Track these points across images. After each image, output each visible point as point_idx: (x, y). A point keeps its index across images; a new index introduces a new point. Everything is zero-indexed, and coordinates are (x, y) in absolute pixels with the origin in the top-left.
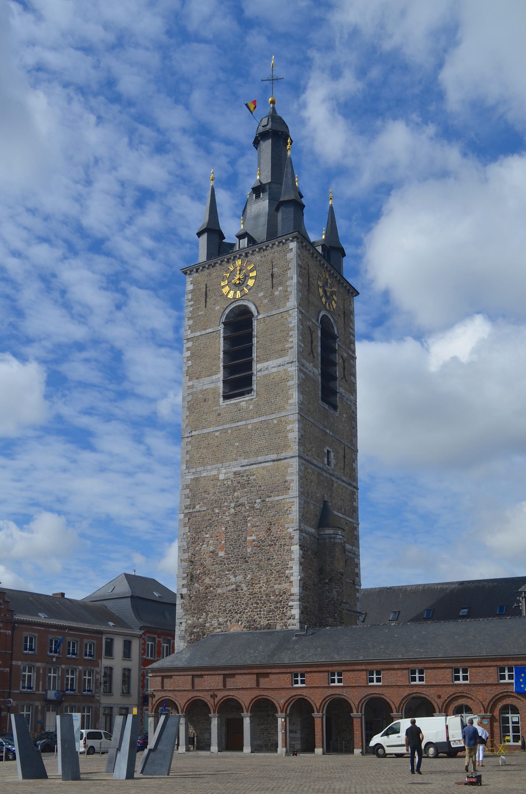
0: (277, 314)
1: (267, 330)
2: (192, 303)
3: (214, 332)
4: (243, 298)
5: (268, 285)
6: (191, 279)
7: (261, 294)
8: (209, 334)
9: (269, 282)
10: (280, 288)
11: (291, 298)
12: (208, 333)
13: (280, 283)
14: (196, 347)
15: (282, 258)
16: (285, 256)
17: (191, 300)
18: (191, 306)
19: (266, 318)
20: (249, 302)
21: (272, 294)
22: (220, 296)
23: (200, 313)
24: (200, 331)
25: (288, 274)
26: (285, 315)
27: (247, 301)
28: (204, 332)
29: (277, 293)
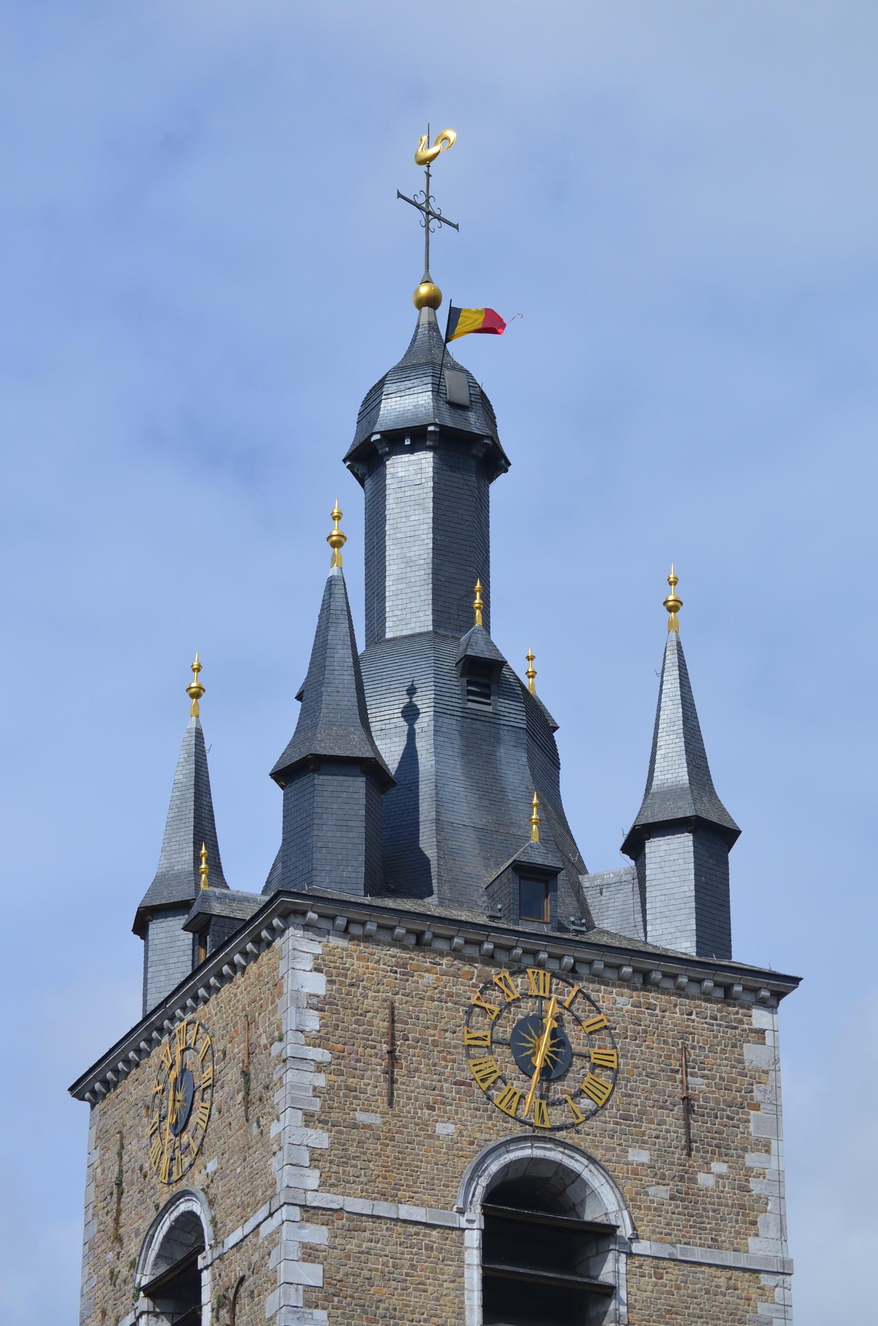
0: (710, 1265)
1: (669, 1312)
2: (322, 1055)
3: (433, 1227)
4: (560, 1135)
5: (668, 1131)
6: (318, 949)
7: (640, 1156)
8: (412, 1229)
9: (673, 1120)
10: (719, 1167)
11: (767, 1226)
12: (405, 1221)
13: (718, 1146)
14: (348, 1257)
15: (723, 1051)
16: (734, 1046)
17: (318, 1041)
18: (320, 1067)
19: (665, 1264)
20: (592, 1167)
21: (687, 1177)
22: (455, 1083)
23: (362, 1117)
24: (366, 1195)
25: (752, 1126)
26: (743, 1281)
27: (585, 1162)
28: (384, 1209)
29: (705, 1180)
